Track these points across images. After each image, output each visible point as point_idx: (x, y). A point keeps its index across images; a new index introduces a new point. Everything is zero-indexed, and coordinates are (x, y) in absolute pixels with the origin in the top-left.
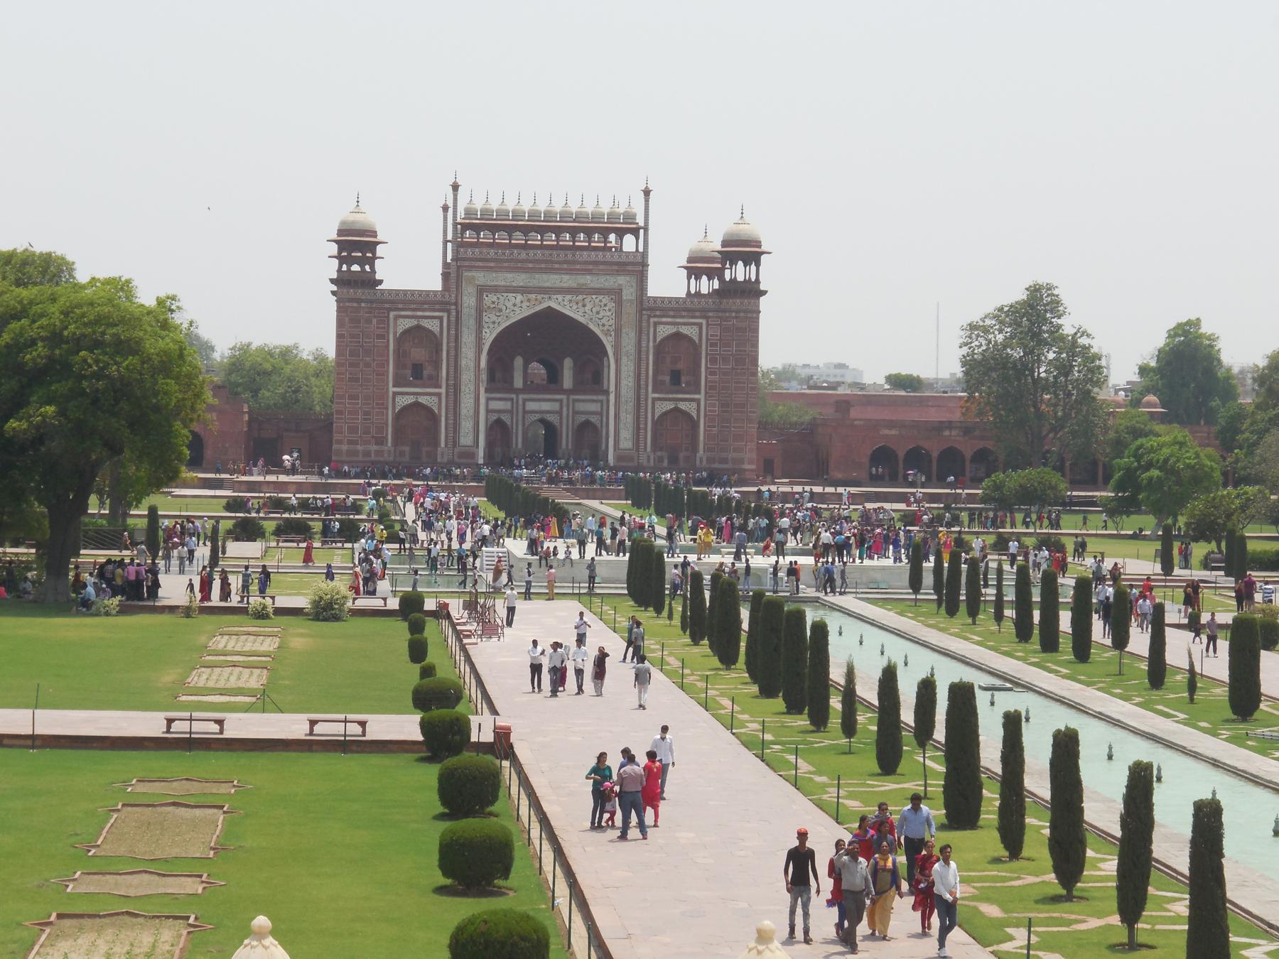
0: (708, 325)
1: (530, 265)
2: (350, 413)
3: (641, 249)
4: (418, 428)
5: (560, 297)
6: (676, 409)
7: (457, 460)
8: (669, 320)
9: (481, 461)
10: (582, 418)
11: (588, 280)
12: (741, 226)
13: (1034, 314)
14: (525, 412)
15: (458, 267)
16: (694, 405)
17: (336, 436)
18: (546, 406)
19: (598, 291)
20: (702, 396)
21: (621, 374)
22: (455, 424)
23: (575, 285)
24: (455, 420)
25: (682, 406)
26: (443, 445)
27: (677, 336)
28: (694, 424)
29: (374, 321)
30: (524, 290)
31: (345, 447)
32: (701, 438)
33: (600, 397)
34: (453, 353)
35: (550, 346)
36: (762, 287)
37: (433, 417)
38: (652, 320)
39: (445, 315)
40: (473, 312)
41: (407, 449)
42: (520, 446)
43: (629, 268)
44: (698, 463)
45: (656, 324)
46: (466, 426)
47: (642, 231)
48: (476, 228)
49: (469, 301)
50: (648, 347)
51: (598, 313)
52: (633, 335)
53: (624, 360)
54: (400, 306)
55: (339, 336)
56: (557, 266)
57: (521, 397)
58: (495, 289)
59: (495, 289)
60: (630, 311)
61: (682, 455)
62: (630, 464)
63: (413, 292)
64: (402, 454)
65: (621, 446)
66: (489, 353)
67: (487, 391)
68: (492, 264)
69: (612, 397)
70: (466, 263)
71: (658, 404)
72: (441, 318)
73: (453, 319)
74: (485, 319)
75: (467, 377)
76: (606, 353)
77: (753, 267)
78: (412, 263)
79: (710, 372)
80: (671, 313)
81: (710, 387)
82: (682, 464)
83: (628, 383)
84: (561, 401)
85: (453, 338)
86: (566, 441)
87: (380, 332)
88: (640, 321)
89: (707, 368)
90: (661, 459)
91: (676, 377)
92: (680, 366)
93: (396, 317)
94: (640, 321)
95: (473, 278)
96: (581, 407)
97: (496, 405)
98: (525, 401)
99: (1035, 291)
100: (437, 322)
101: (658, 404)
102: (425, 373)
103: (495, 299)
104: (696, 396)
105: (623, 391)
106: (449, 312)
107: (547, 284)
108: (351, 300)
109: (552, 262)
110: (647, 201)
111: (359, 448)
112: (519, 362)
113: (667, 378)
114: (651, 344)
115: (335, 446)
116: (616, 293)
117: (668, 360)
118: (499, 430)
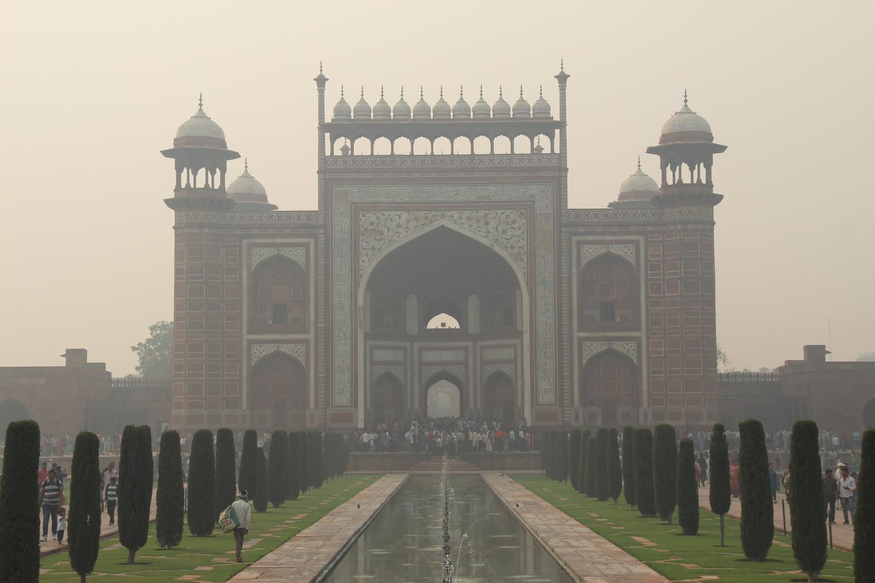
0: (646, 242)
1: (417, 175)
3: (557, 150)
5: (456, 214)
6: (610, 352)
8: (596, 238)
9: (361, 425)
16: (633, 345)
19: (505, 205)
20: (643, 334)
21: (537, 309)
25: (618, 346)
26: (312, 405)
27: (608, 259)
30: (409, 207)
32: (645, 387)
33: (513, 341)
36: (716, 191)
39: (312, 242)
42: (416, 406)
44: (641, 419)
46: (342, 380)
49: (341, 223)
51: (504, 232)
54: (255, 232)
55: (178, 271)
65: (541, 400)
66: (369, 288)
67: (367, 336)
69: (526, 338)
71: (586, 345)
72: (306, 246)
73: (321, 246)
74: (362, 244)
76: (517, 285)
77: (703, 170)
80: (599, 229)
84: (466, 349)
89: (647, 297)
93: (251, 246)
97: (381, 355)
100: (301, 251)
101: (586, 345)
103: (374, 219)
104: (636, 334)
106: (315, 237)
107: (438, 199)
112: (412, 302)
114: (574, 269)
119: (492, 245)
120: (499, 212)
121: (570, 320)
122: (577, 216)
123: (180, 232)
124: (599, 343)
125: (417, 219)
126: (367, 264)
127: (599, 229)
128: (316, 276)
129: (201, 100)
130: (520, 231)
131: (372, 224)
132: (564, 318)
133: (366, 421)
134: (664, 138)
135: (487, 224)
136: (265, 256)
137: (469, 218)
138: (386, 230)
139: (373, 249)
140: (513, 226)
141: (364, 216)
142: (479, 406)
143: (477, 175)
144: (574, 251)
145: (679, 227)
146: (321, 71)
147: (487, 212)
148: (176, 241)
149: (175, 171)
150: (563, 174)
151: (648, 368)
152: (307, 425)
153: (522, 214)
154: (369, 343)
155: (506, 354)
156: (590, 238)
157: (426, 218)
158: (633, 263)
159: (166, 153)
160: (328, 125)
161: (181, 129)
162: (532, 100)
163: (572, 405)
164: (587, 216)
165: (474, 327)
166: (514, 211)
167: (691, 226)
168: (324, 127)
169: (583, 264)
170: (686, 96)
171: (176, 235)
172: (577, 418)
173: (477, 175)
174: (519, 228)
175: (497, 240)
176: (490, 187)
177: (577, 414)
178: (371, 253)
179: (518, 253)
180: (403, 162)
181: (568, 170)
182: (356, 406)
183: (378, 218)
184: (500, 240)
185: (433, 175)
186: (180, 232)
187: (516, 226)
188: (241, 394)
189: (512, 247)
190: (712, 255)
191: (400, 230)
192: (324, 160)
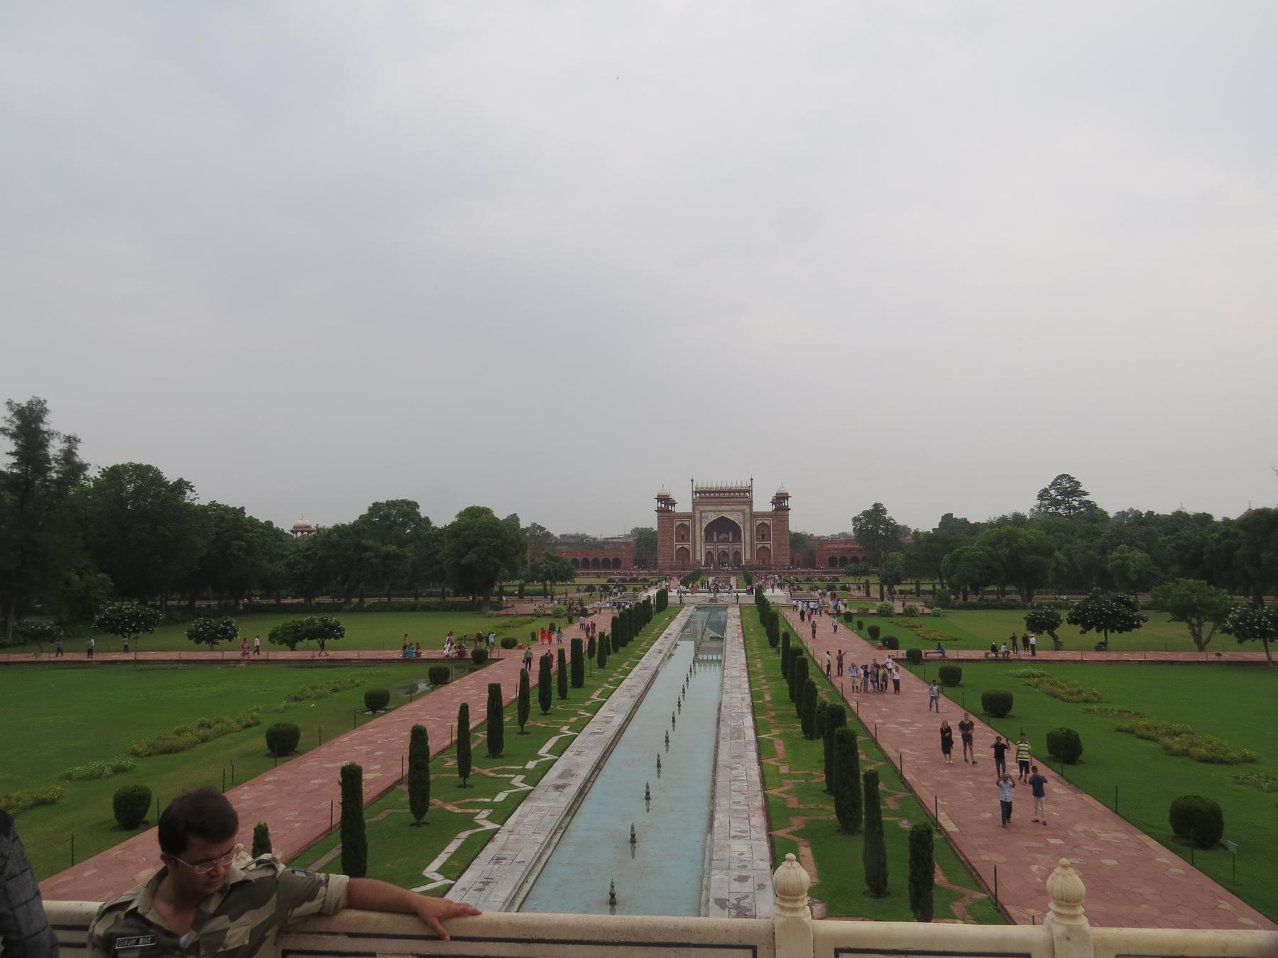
4: (684, 553)
13: (878, 510)
21: (746, 536)
35: (723, 527)
37: (688, 551)
46: (698, 554)
48: (700, 492)
49: (698, 515)
60: (748, 516)
75: (698, 539)
78: (683, 505)
83: (748, 539)
86: (731, 557)
91: (763, 537)
99: (877, 506)
116: (743, 511)
118: (709, 554)
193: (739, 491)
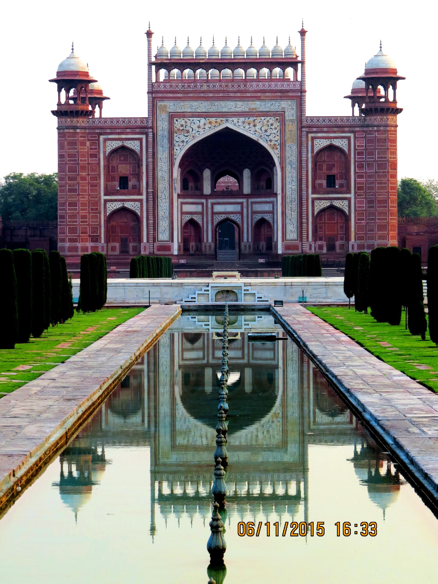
0: (355, 138)
1: (211, 95)
2: (70, 217)
5: (235, 120)
7: (156, 252)
9: (176, 253)
10: (258, 217)
11: (258, 105)
12: (380, 58)
14: (213, 213)
15: (154, 98)
16: (346, 202)
17: (60, 236)
18: (230, 208)
19: (265, 114)
20: (352, 196)
21: (286, 179)
22: (154, 223)
23: (247, 110)
24: (154, 221)
25: (337, 204)
26: (145, 240)
27: (331, 148)
28: (347, 218)
29: (88, 143)
31: (67, 244)
32: (353, 229)
33: (271, 199)
34: (151, 167)
36: (399, 106)
37: (137, 218)
38: (310, 135)
39: (144, 137)
40: (166, 133)
41: (117, 245)
43: (290, 94)
45: (313, 138)
46: (163, 224)
47: (299, 65)
49: (162, 125)
50: (307, 158)
51: (266, 131)
52: (295, 148)
53: (288, 168)
54: (108, 131)
55: (61, 156)
56: (232, 95)
57: (210, 201)
58: (183, 115)
59: (183, 115)
60: (292, 128)
61: (338, 243)
62: (296, 252)
63: (118, 120)
64: (113, 249)
65: (288, 237)
67: (179, 196)
68: (180, 95)
70: (160, 95)
71: (316, 203)
73: (150, 140)
74: (176, 139)
75: (163, 186)
76: (274, 165)
79: (358, 176)
80: (325, 129)
81: (358, 188)
82: (338, 250)
83: (292, 186)
84: (242, 203)
85: (150, 155)
87: (93, 152)
88: (301, 137)
89: (355, 172)
90: (321, 247)
91: (331, 181)
92: (335, 171)
93: (105, 140)
94: (301, 137)
95: (165, 106)
96: (257, 208)
97: (187, 208)
98: (213, 204)
100: (138, 143)
101: (316, 203)
102: (130, 184)
103: (183, 122)
104: (348, 196)
105: (288, 193)
106: (147, 134)
107: (224, 110)
108: (68, 128)
109: (228, 92)
110: (303, 40)
111: (79, 245)
112: (207, 174)
113: (324, 182)
114: (310, 155)
115: (60, 244)
116: (280, 116)
117: (325, 167)
119: (258, 140)
120: (263, 118)
121: (307, 187)
122: (312, 121)
123: (61, 131)
124: (325, 201)
125: (210, 123)
126: (179, 152)
127: (325, 129)
128: (147, 159)
129: (73, 46)
130: (276, 131)
131: (182, 126)
132: (303, 186)
133: (179, 250)
134: (367, 72)
135: (255, 126)
136: (114, 147)
137: (244, 122)
138: (191, 130)
139: (183, 142)
140: (271, 127)
141: (177, 121)
142: (250, 240)
143: (249, 95)
144: (310, 143)
145: (375, 128)
146: (149, 27)
147: (255, 118)
148: (59, 137)
149: (57, 93)
150: (303, 94)
151: (355, 217)
152: (142, 253)
153: (277, 119)
154: (180, 200)
155: (267, 207)
156: (320, 135)
157: (216, 122)
158: (347, 151)
159: (50, 81)
160: (154, 64)
161: (61, 65)
162: (283, 46)
163: (308, 240)
164: (318, 121)
165: (247, 189)
166: (272, 118)
167: (382, 128)
168: (150, 64)
169: (315, 151)
170: (381, 44)
171: (59, 134)
172: (310, 249)
173: (249, 95)
174: (275, 128)
175: (261, 136)
176: (258, 103)
177: (310, 245)
178: (181, 144)
179: (275, 145)
180: (201, 86)
181: (305, 92)
182: (172, 241)
183: (186, 122)
184: (263, 136)
185: (221, 95)
186: (61, 131)
187: (273, 127)
188: (100, 233)
189: (271, 141)
190: (396, 146)
191: (200, 130)
192: (151, 85)
193: (271, 64)
